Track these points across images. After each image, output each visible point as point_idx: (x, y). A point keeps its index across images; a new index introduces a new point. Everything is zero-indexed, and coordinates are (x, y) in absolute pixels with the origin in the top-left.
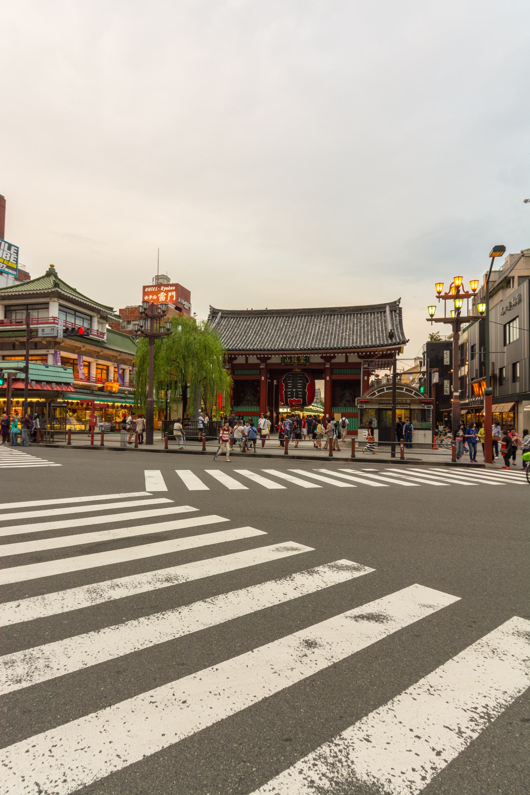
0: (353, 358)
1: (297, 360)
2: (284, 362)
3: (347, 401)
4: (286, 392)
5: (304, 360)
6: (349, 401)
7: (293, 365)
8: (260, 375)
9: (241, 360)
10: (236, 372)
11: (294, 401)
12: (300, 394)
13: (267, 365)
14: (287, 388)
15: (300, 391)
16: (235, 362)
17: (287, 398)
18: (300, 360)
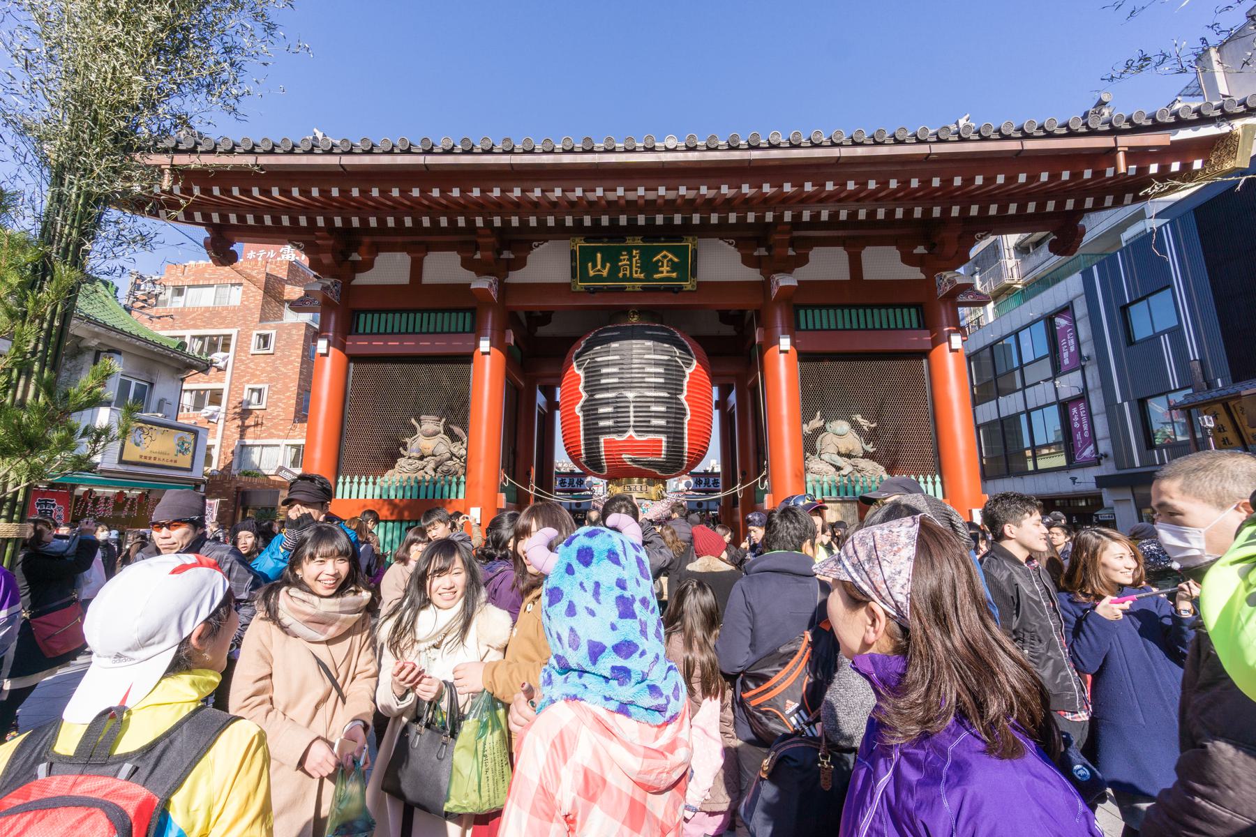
0: (884, 264)
1: (643, 268)
2: (585, 277)
3: (839, 454)
4: (590, 410)
5: (674, 267)
6: (849, 456)
7: (623, 289)
8: (477, 332)
9: (390, 269)
10: (365, 322)
11: (631, 446)
12: (658, 416)
13: (504, 288)
14: (592, 387)
15: (658, 401)
16: (362, 279)
17: (593, 432)
18: (656, 268)
